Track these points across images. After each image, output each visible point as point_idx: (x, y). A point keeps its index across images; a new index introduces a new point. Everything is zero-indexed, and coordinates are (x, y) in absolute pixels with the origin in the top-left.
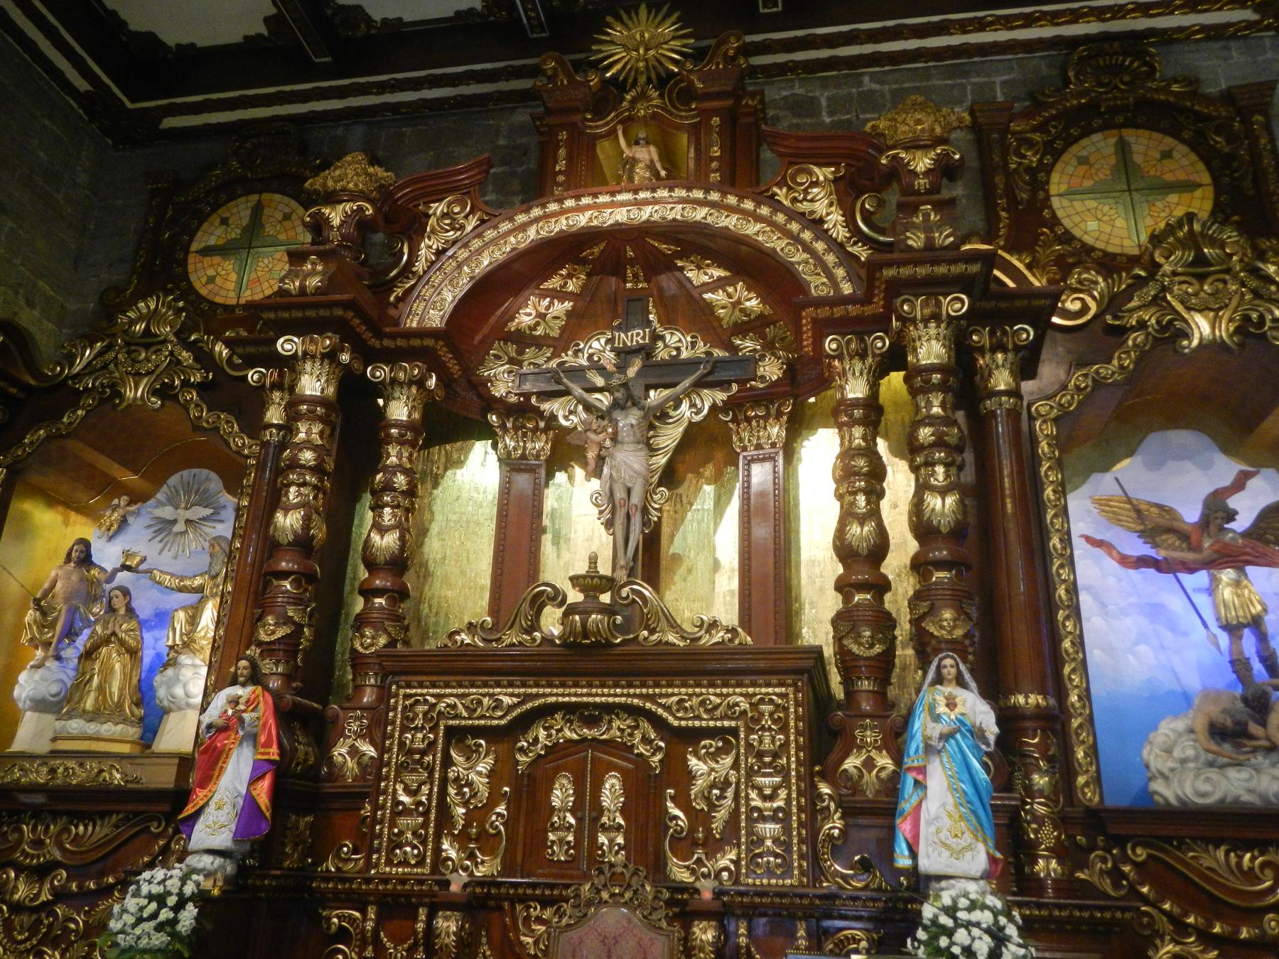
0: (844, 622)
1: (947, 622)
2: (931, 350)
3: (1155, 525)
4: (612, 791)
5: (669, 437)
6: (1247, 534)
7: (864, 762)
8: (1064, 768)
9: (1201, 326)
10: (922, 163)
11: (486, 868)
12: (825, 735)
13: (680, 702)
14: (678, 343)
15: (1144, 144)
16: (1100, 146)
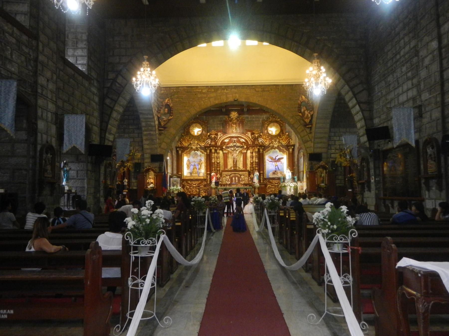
0: (251, 167)
1: (257, 168)
2: (257, 150)
3: (272, 158)
4: (237, 178)
5: (238, 152)
6: (278, 160)
7: (252, 176)
8: (263, 176)
9: (276, 146)
10: (257, 135)
11: (229, 183)
12: (249, 175)
13: (241, 173)
14: (238, 144)
15: (276, 124)
16: (272, 124)
